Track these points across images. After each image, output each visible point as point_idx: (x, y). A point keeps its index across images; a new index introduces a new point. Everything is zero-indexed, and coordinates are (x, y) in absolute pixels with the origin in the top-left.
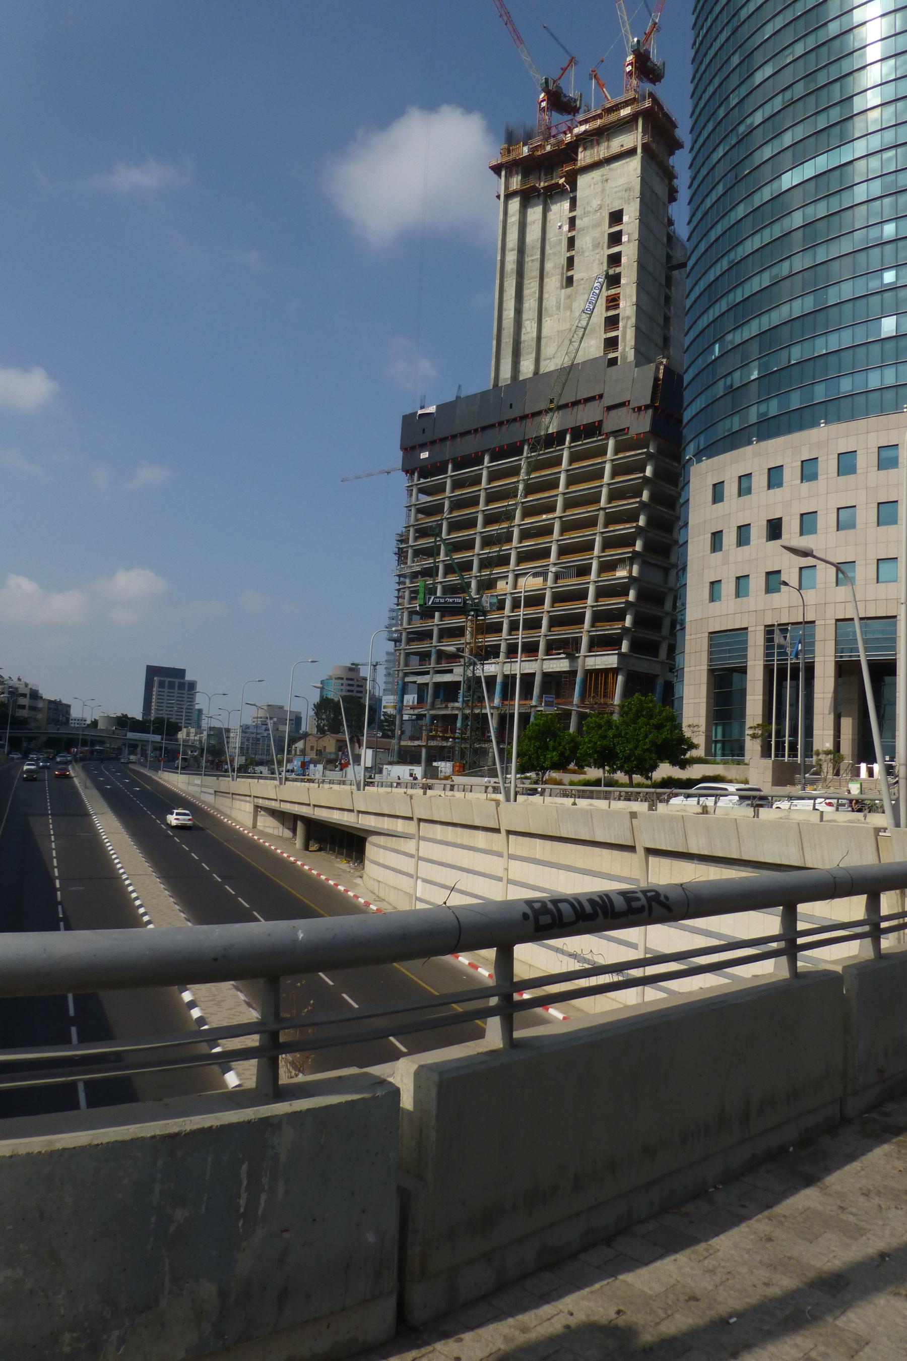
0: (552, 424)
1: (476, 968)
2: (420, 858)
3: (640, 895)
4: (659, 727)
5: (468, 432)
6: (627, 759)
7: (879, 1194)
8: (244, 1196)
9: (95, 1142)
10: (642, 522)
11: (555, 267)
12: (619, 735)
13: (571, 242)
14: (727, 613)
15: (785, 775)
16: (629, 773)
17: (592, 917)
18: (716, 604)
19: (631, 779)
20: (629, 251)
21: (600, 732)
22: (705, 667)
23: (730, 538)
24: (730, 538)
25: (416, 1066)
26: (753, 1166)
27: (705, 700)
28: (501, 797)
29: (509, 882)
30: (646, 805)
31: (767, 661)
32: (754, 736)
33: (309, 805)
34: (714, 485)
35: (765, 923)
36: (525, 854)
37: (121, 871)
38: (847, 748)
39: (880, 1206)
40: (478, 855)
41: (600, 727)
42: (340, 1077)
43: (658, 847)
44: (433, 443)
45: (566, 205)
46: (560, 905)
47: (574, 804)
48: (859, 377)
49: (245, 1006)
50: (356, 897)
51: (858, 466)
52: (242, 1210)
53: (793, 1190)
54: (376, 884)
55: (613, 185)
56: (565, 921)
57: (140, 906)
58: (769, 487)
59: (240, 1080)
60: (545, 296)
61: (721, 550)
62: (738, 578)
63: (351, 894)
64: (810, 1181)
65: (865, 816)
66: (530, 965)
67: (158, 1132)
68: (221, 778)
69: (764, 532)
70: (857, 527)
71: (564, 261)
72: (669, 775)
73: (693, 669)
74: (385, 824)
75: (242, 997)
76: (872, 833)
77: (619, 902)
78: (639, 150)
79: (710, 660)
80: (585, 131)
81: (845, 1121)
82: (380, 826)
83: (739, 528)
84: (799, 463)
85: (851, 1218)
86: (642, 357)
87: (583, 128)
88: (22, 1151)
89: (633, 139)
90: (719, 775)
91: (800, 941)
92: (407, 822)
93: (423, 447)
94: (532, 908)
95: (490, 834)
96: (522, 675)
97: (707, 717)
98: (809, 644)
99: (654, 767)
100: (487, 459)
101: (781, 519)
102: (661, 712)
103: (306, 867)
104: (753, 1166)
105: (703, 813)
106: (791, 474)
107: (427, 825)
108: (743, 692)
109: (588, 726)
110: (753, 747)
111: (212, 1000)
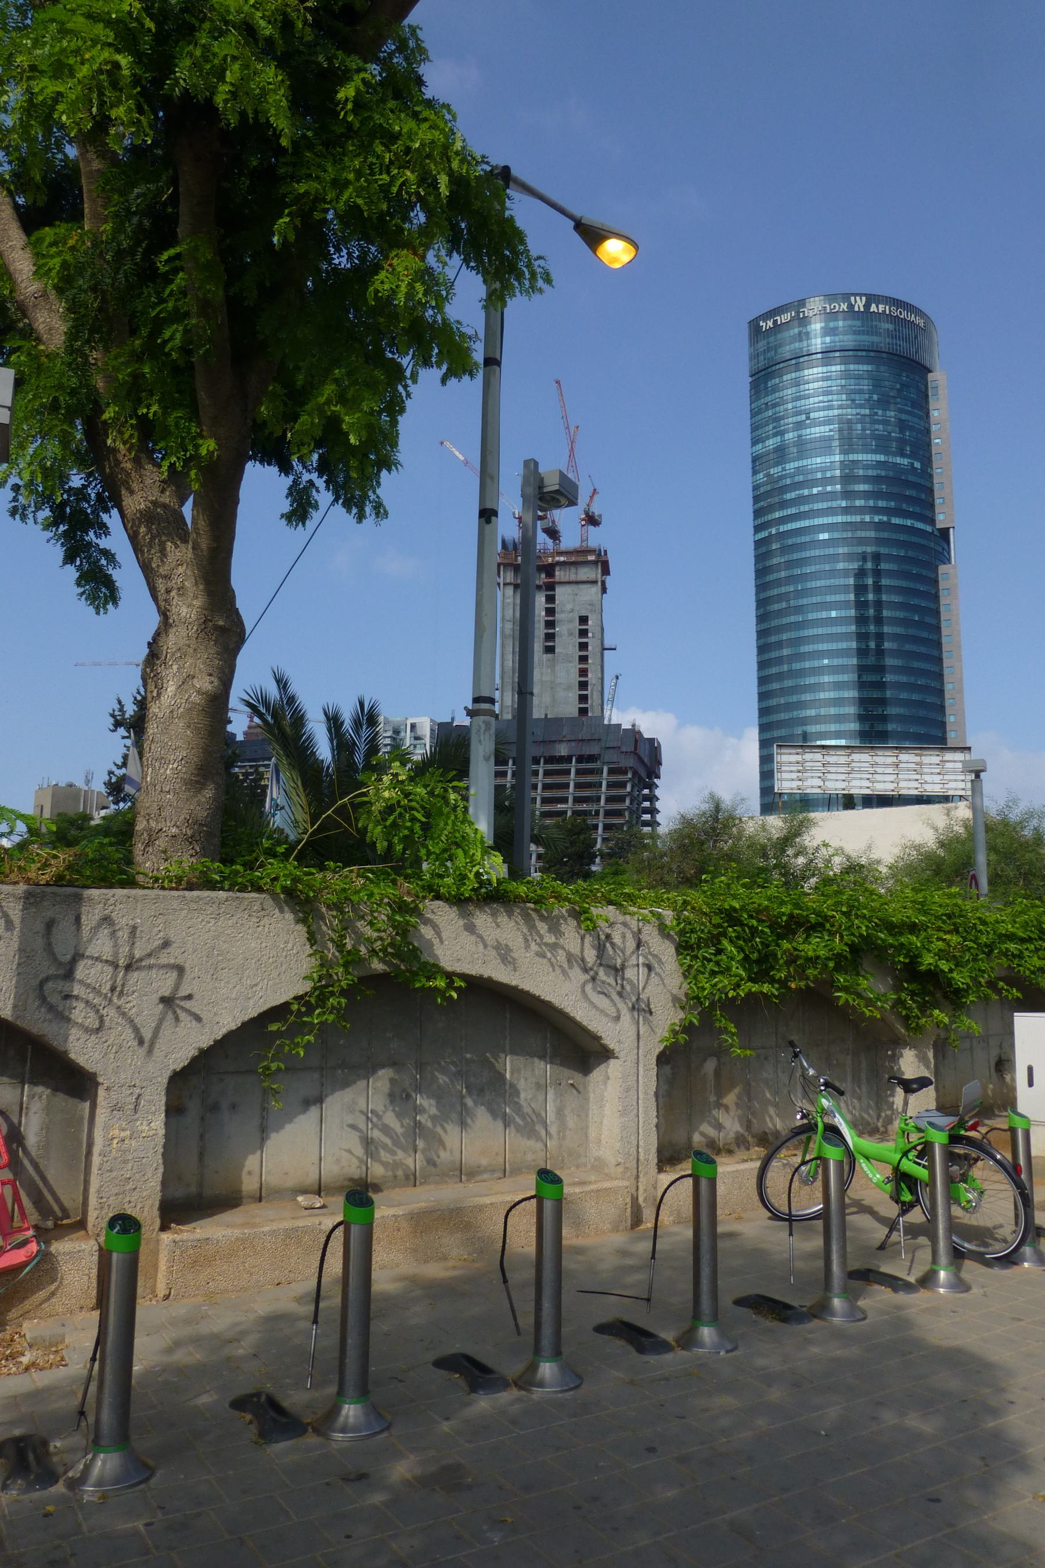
0: (563, 750)
71: (542, 636)
100: (511, 762)
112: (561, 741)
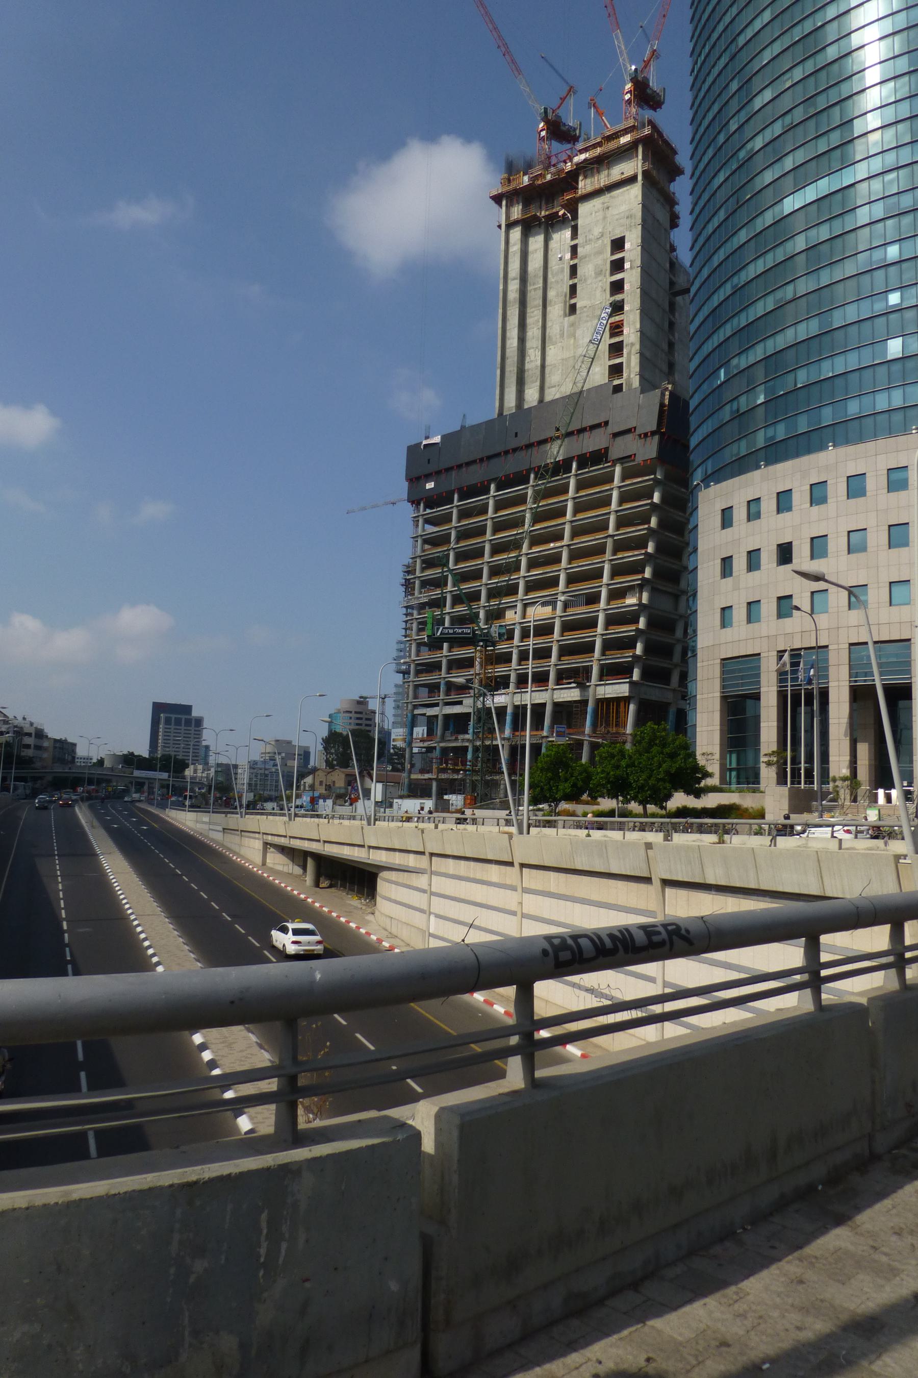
0: (556, 452)
1: (492, 1005)
2: (432, 894)
3: (661, 929)
4: (673, 756)
5: (474, 462)
6: (641, 788)
7: (911, 1232)
8: (264, 1245)
9: (113, 1192)
10: (650, 549)
11: (557, 295)
12: (632, 765)
13: (574, 270)
14: (738, 639)
15: (802, 802)
16: (644, 803)
17: (613, 952)
18: (728, 630)
19: (645, 809)
20: (632, 277)
21: (613, 762)
22: (718, 694)
23: (739, 564)
24: (739, 564)
25: (436, 1109)
26: (781, 1205)
27: (718, 727)
28: (513, 830)
29: (524, 916)
30: (661, 835)
31: (780, 687)
32: (769, 764)
33: (319, 841)
34: (723, 510)
35: (787, 955)
36: (539, 887)
37: (129, 911)
38: (863, 773)
39: (913, 1245)
40: (492, 890)
41: (612, 756)
42: (360, 1121)
43: (675, 878)
44: (438, 473)
45: (568, 233)
46: (580, 940)
47: (589, 835)
48: (866, 400)
49: (256, 1049)
50: (368, 934)
51: (868, 488)
52: (262, 1260)
53: (823, 1230)
54: (388, 921)
55: (614, 213)
56: (585, 956)
57: (149, 947)
58: (778, 512)
59: (253, 1123)
60: (549, 324)
61: (731, 575)
62: (749, 604)
63: (363, 931)
64: (840, 1220)
65: (886, 844)
66: (547, 1001)
67: (176, 1181)
68: (229, 815)
69: (774, 557)
70: (868, 549)
72: (684, 804)
73: (705, 696)
74: (397, 859)
75: (253, 1038)
76: (892, 859)
77: (640, 937)
78: (640, 178)
79: (723, 687)
80: (585, 160)
81: (874, 1157)
82: (391, 861)
83: (749, 553)
84: (808, 487)
85: (884, 1259)
86: (647, 384)
87: (583, 157)
88: (39, 1202)
89: (634, 166)
90: (734, 804)
91: (824, 973)
92: (419, 856)
93: (428, 477)
94: (552, 944)
95: (503, 867)
96: (532, 705)
97: (721, 745)
98: (823, 670)
99: (668, 797)
100: (493, 486)
101: (791, 543)
102: (674, 740)
103: (317, 905)
104: (781, 1205)
105: (719, 843)
106: (800, 498)
107: (439, 859)
108: (757, 719)
109: (601, 756)
110: (768, 774)
111: (223, 1043)
112: (552, 439)
